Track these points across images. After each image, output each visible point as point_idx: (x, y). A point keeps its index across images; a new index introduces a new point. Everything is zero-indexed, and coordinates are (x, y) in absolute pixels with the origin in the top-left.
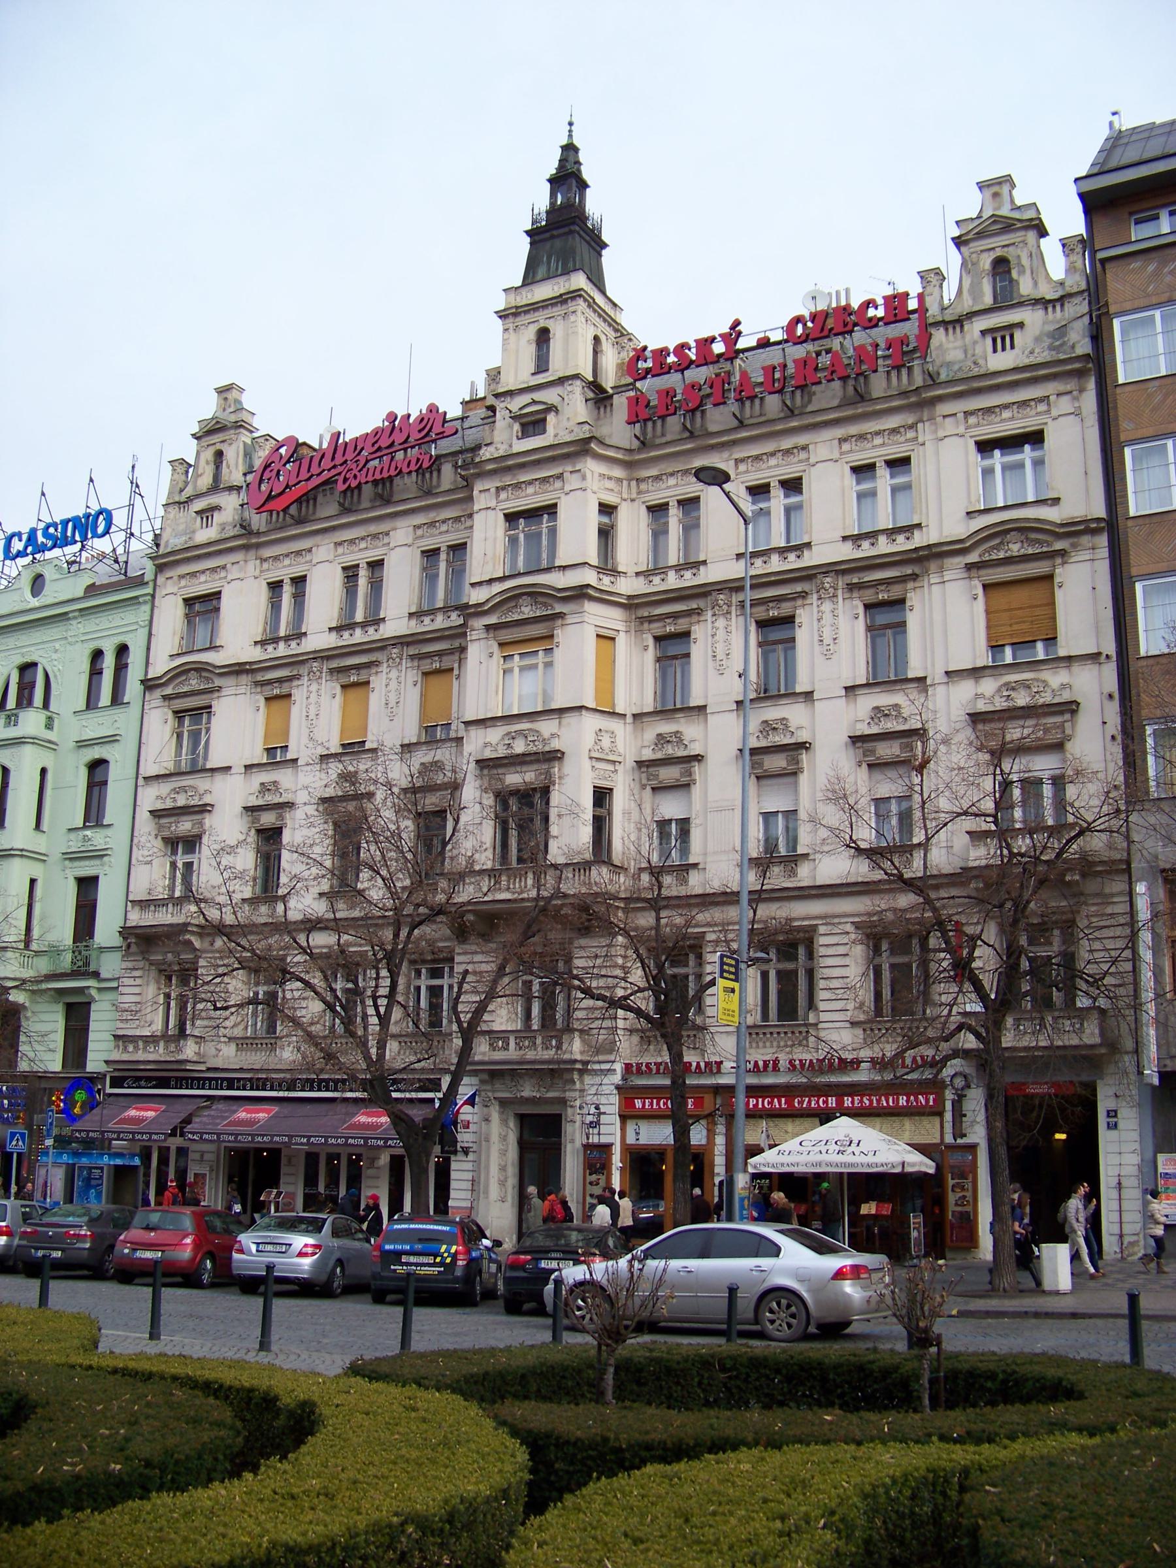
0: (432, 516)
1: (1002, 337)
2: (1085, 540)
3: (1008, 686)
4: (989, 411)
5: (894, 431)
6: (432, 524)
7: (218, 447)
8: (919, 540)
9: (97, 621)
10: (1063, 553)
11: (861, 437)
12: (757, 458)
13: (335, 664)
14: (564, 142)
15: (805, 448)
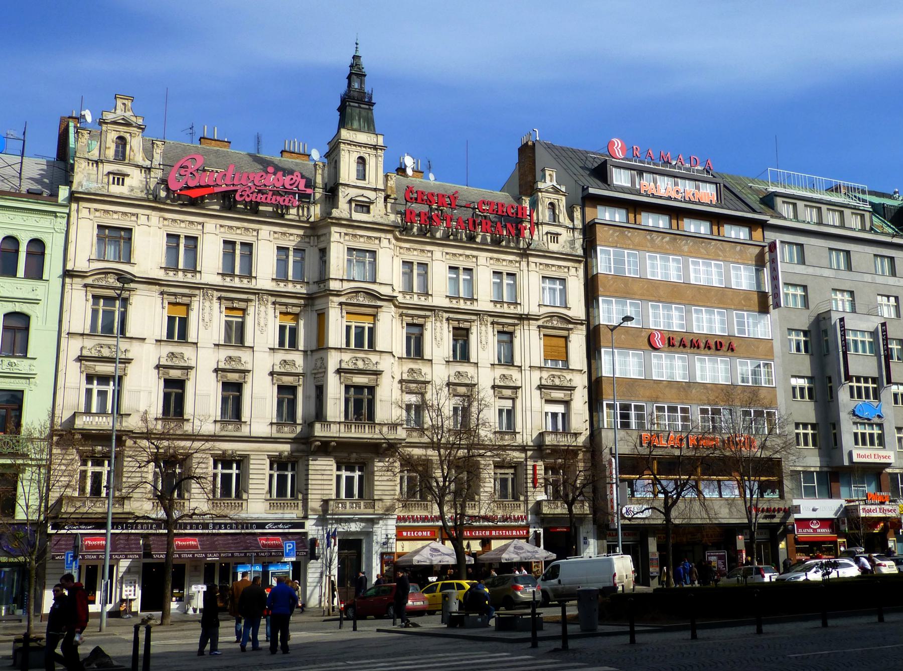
0: (284, 230)
1: (555, 236)
2: (579, 326)
3: (554, 376)
4: (547, 265)
5: (511, 261)
6: (284, 234)
7: (122, 134)
8: (519, 310)
9: (11, 217)
10: (571, 329)
11: (498, 260)
12: (454, 255)
13: (224, 294)
14: (353, 53)
15: (477, 257)
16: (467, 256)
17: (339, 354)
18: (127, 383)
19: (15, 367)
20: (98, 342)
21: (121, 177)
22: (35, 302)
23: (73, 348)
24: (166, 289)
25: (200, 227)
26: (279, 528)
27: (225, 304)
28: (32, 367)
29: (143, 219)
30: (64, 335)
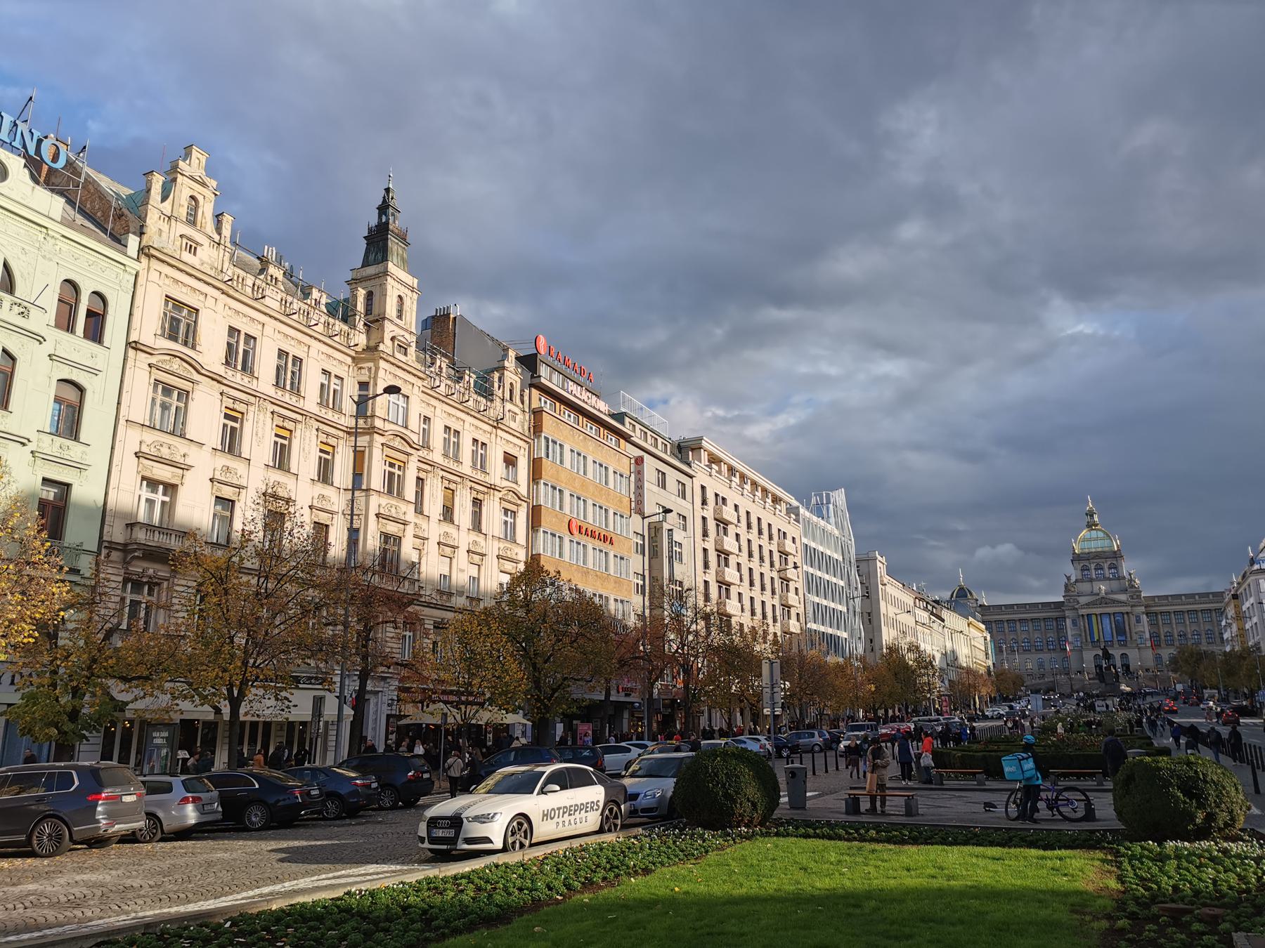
0: (330, 351)
5: (485, 431)
16: (458, 418)
17: (377, 497)
21: (194, 245)
22: (94, 372)
23: (131, 439)
24: (226, 389)
25: (260, 327)
26: (311, 684)
27: (279, 421)
28: (84, 456)
29: (210, 302)
30: (122, 422)
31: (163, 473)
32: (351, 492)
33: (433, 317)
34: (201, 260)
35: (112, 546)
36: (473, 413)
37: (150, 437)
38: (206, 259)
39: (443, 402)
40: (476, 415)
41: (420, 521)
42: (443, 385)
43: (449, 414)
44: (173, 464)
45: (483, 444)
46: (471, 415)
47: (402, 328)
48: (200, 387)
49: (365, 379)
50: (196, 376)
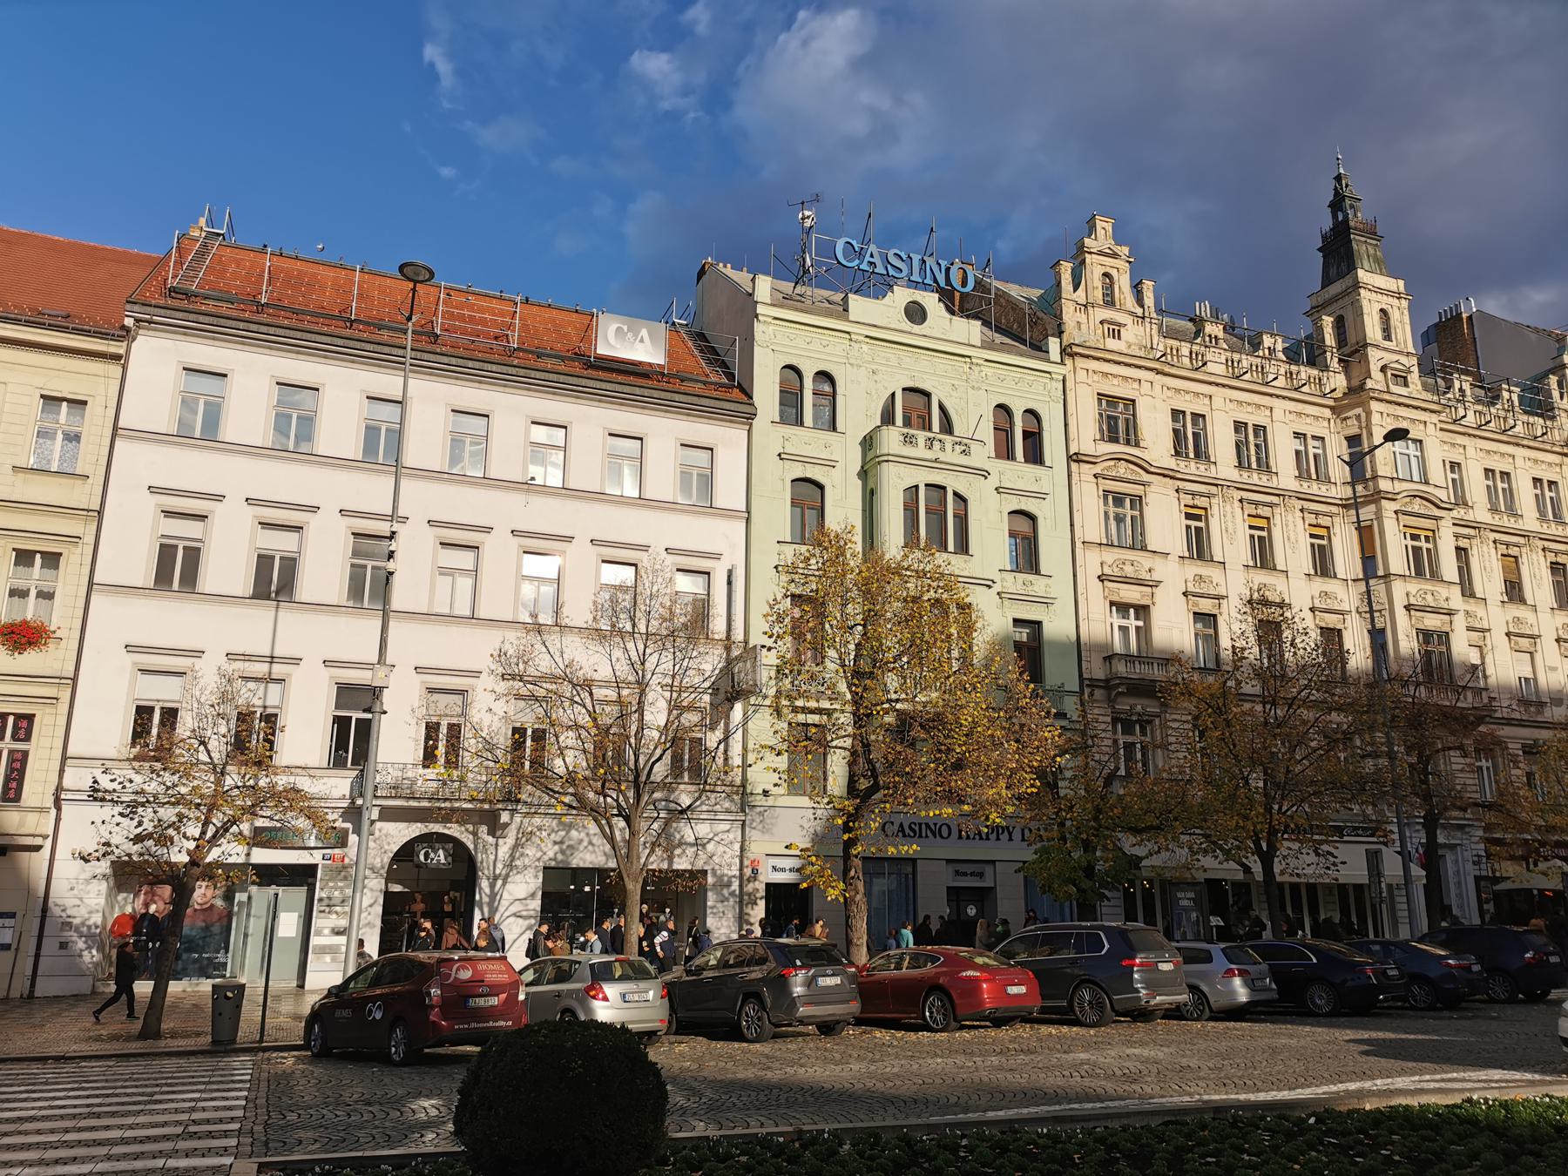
0: (1300, 407)
16: (1503, 455)
17: (1402, 583)
18: (1156, 613)
19: (1030, 588)
20: (1117, 556)
21: (1117, 328)
22: (1041, 496)
23: (1092, 562)
24: (1182, 484)
25: (1207, 401)
26: (1358, 835)
27: (1250, 509)
28: (1048, 589)
29: (1146, 386)
30: (1079, 544)
31: (1131, 594)
32: (1364, 583)
33: (1436, 325)
34: (1127, 342)
35: (1094, 684)
36: (1525, 442)
37: (1111, 556)
38: (1132, 339)
39: (1475, 436)
40: (1531, 444)
41: (1472, 606)
42: (1470, 414)
43: (1488, 452)
44: (1140, 583)
45: (1551, 483)
46: (1523, 446)
47: (1394, 352)
48: (1152, 488)
49: (1354, 431)
50: (1146, 477)
